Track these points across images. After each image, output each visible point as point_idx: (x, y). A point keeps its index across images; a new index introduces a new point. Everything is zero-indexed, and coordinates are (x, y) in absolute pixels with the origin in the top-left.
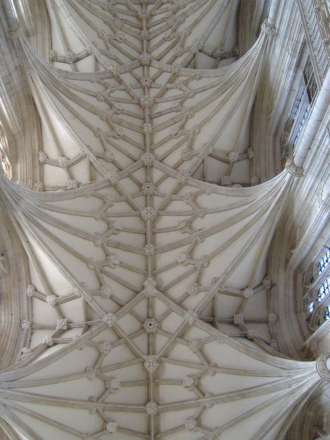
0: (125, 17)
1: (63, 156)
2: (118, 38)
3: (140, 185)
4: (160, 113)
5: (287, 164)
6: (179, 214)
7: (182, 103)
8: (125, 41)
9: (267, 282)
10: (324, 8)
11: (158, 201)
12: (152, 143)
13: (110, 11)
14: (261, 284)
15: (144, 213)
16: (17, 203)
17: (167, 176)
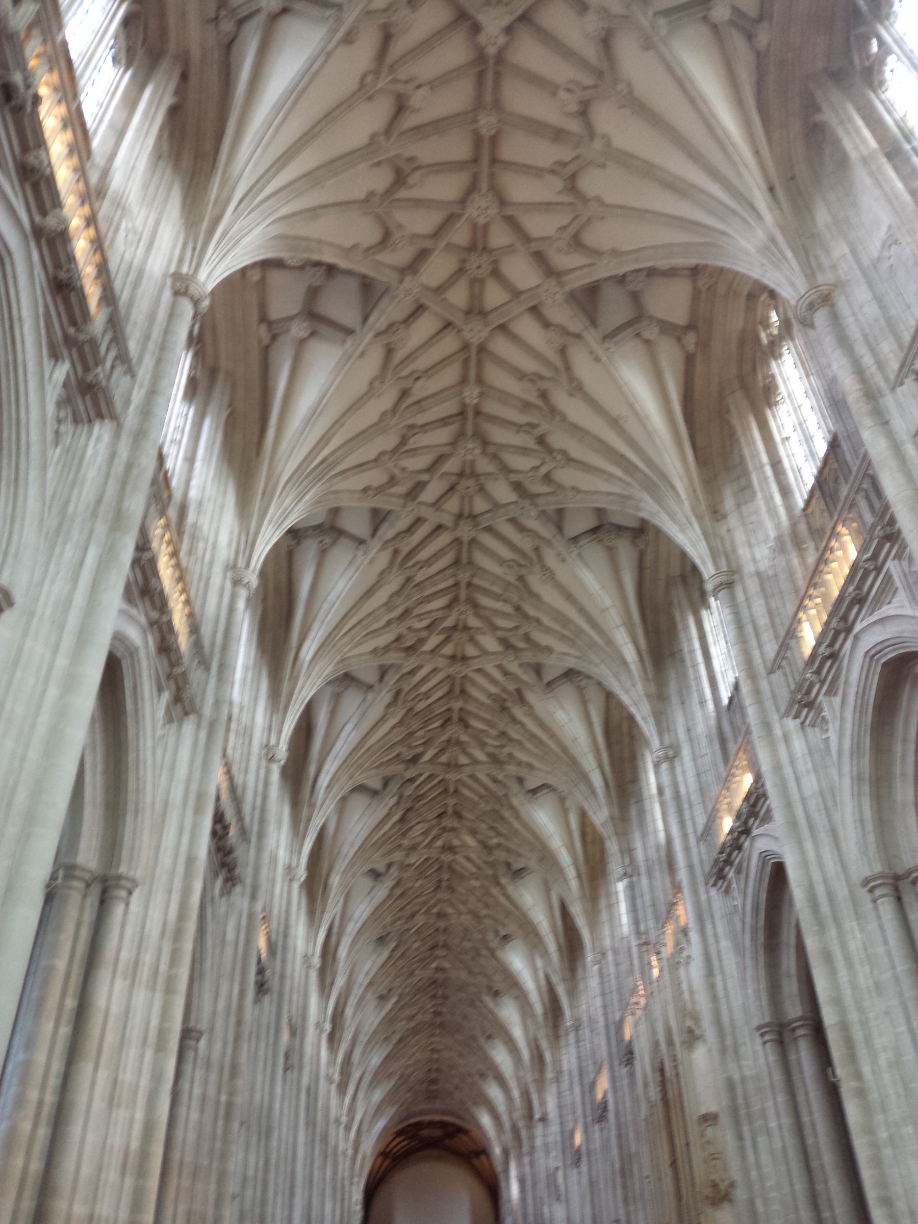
0: (499, 606)
1: (647, 342)
2: (516, 568)
3: (496, 273)
4: (446, 425)
5: (206, 303)
6: (419, 203)
7: (404, 441)
8: (502, 562)
9: (227, 26)
10: (155, 615)
11: (460, 235)
12: (466, 361)
13: (526, 617)
14: (241, 22)
15: (493, 211)
16: (773, 240)
17: (440, 290)
